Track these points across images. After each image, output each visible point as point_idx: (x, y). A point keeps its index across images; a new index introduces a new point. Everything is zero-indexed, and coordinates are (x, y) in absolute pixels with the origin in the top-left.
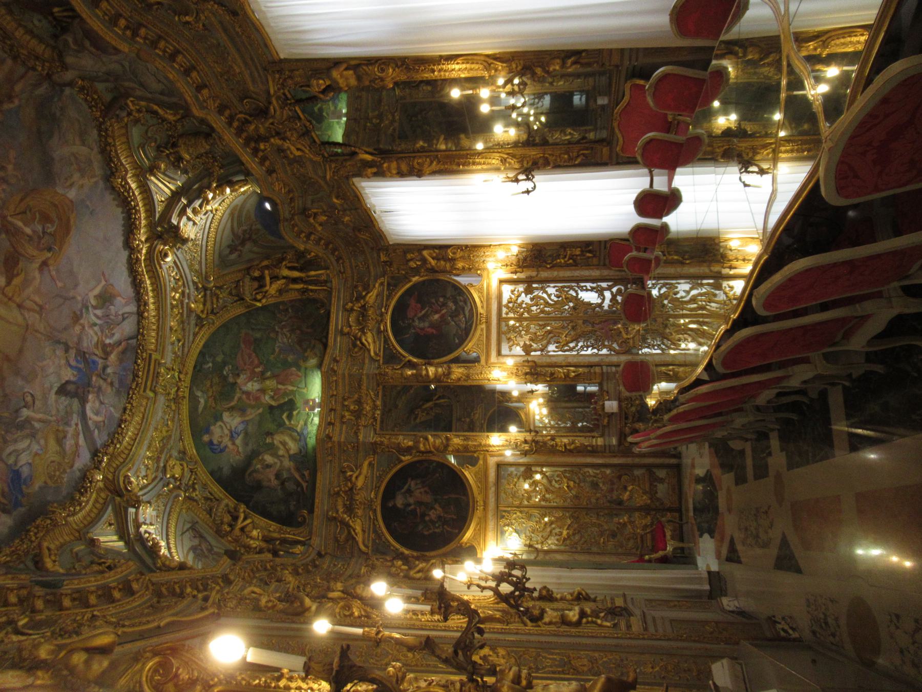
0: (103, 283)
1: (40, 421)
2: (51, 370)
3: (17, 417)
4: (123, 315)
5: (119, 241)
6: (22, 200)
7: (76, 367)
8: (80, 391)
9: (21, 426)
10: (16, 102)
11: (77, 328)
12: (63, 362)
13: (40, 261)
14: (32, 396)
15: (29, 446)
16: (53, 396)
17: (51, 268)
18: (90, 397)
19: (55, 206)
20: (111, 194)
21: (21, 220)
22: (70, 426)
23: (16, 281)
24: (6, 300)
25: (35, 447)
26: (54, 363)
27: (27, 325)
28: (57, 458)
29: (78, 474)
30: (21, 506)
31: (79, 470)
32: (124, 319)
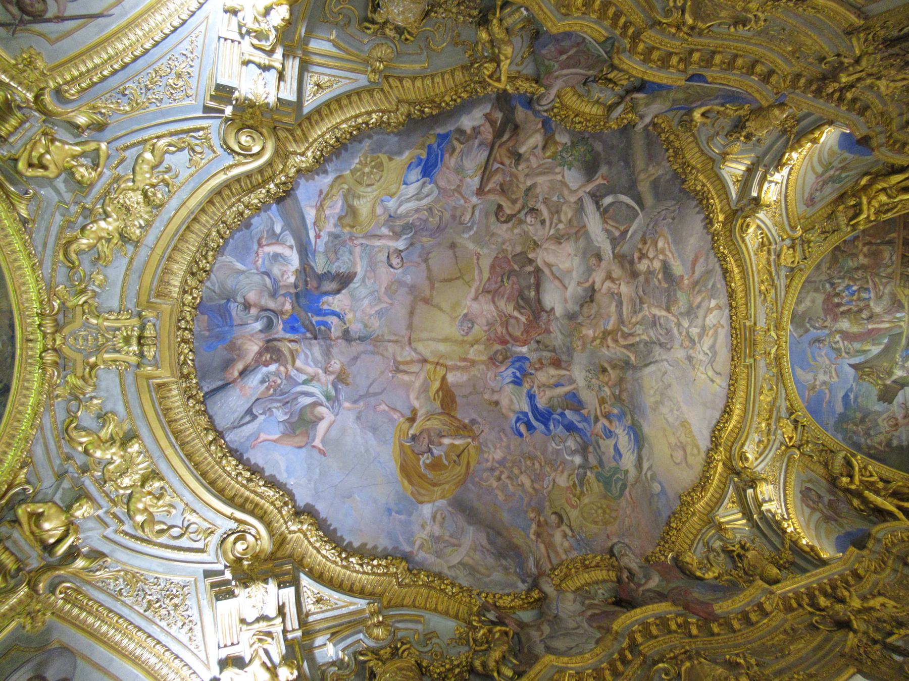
0: (317, 443)
1: (380, 237)
2: (366, 302)
3: (412, 237)
4: (255, 417)
5: (322, 508)
6: (468, 463)
7: (325, 315)
8: (313, 284)
9: (407, 227)
10: (533, 537)
11: (336, 365)
12: (350, 316)
13: (417, 421)
14: (391, 266)
15: (400, 206)
16: (360, 269)
17: (402, 420)
18: (292, 279)
19: (435, 485)
20: (385, 549)
21: (458, 446)
22: (330, 234)
23: (436, 385)
24: (441, 361)
25: (392, 204)
26: (363, 312)
27: (410, 344)
28: (361, 190)
29: (330, 167)
30: (439, 135)
31: (325, 172)
32: (249, 412)
